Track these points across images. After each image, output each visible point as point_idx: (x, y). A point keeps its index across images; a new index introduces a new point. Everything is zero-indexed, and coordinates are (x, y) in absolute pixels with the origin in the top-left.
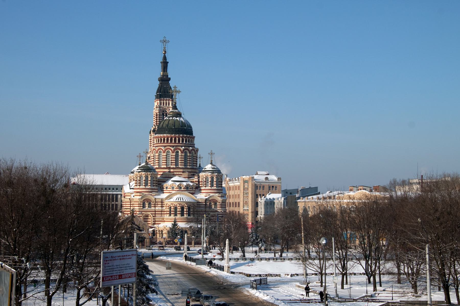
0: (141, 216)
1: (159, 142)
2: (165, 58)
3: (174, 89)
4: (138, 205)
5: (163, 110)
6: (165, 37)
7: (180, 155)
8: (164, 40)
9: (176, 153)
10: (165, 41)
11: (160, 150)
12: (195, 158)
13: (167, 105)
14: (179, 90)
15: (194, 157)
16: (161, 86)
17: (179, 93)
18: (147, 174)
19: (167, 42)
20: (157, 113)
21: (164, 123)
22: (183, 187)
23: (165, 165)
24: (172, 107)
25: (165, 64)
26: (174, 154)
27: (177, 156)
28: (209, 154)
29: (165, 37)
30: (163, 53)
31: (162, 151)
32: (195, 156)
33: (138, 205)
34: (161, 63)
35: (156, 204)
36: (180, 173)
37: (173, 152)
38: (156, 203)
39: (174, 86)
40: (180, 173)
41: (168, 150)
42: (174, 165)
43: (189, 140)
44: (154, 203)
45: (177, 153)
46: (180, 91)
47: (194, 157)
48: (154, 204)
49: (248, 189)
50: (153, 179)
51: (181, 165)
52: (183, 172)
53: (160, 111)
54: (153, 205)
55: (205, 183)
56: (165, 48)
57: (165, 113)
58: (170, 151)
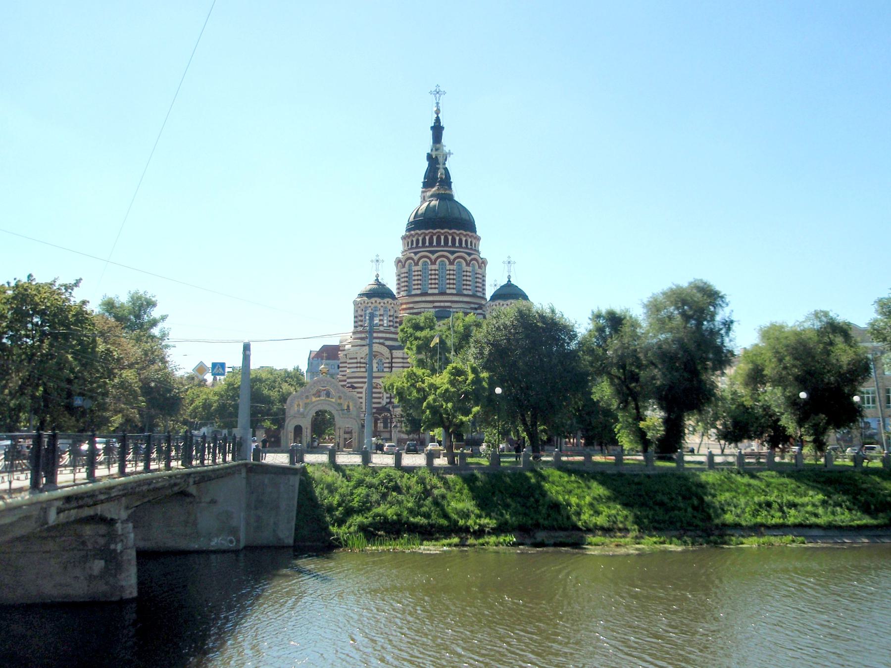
0: (362, 388)
2: (438, 120)
4: (355, 365)
8: (436, 91)
10: (438, 93)
12: (480, 276)
15: (476, 274)
18: (376, 302)
23: (417, 289)
25: (437, 130)
33: (355, 365)
35: (392, 363)
38: (393, 360)
42: (435, 288)
43: (466, 241)
44: (387, 361)
45: (442, 265)
47: (476, 274)
48: (389, 363)
50: (389, 313)
54: (387, 365)
56: (438, 103)
58: (428, 260)
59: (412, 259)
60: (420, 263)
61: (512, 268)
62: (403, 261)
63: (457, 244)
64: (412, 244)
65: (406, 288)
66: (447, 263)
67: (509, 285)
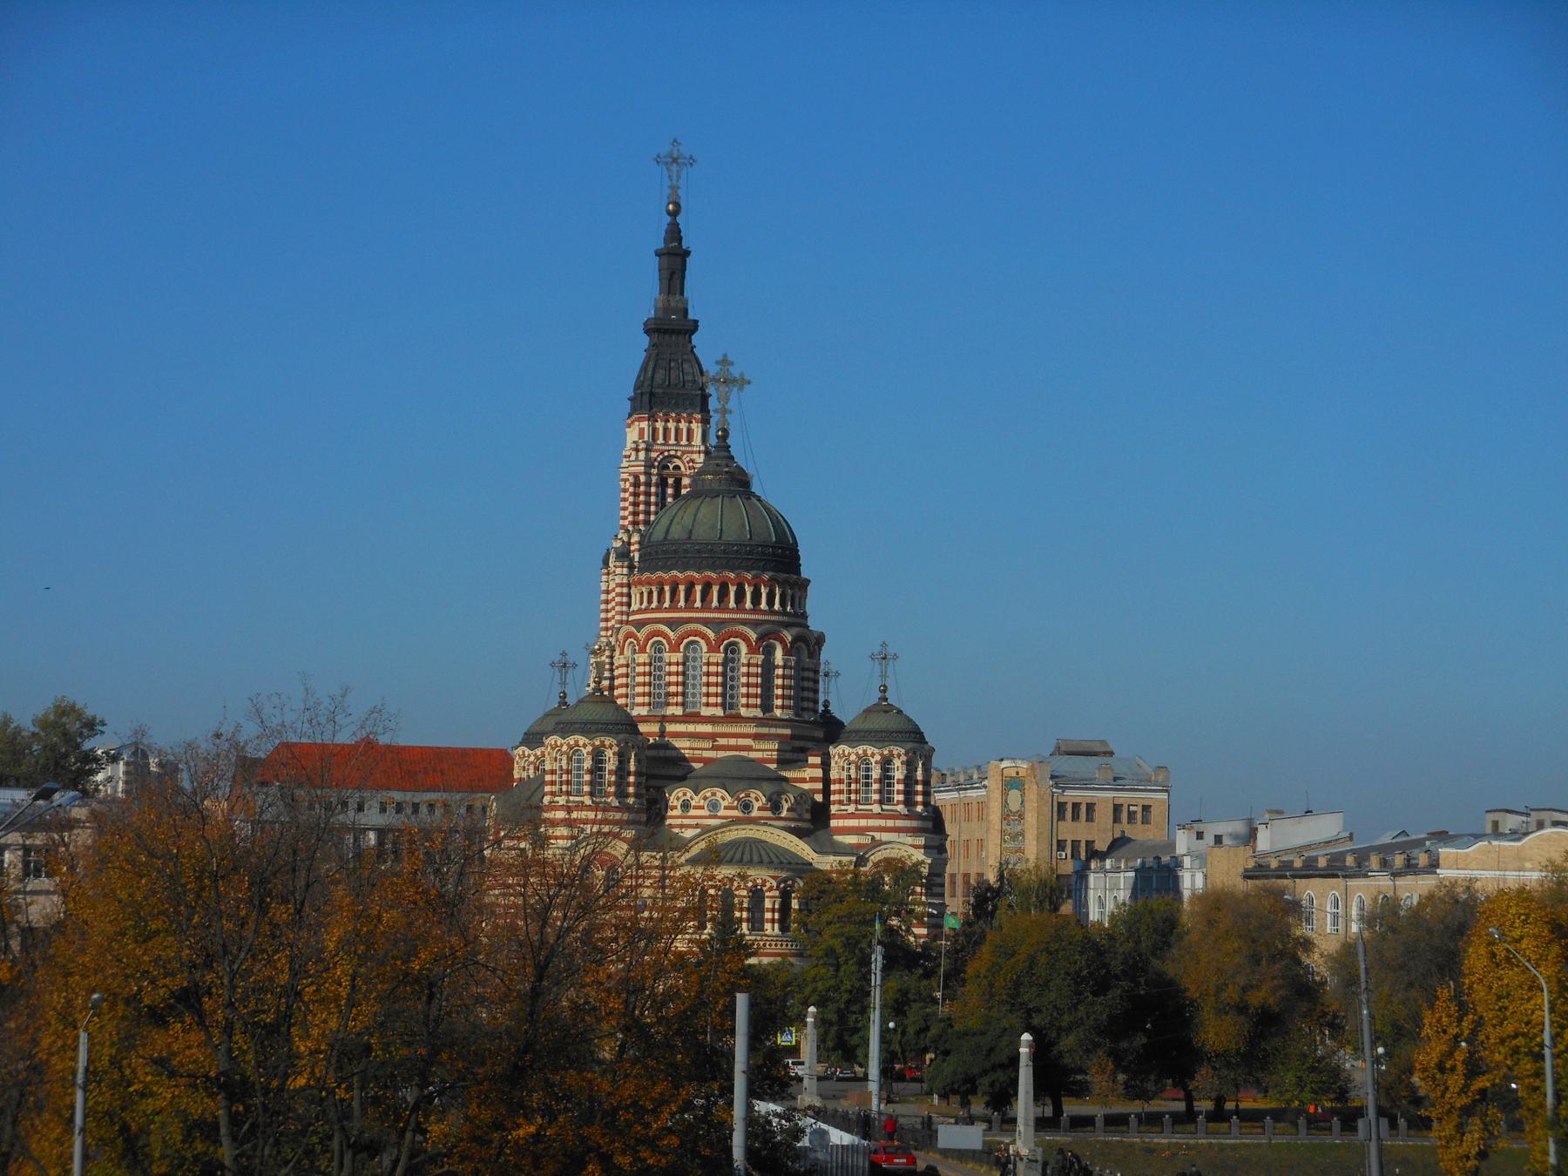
1: (650, 601)
2: (674, 233)
3: (718, 367)
5: (663, 463)
6: (675, 141)
7: (744, 660)
9: (726, 653)
10: (675, 160)
11: (655, 639)
12: (811, 675)
13: (684, 442)
14: (742, 374)
15: (804, 669)
16: (657, 355)
17: (741, 389)
19: (686, 165)
20: (636, 477)
21: (674, 517)
22: (757, 805)
24: (702, 448)
25: (674, 259)
26: (719, 657)
27: (729, 662)
28: (872, 657)
29: (675, 141)
30: (669, 213)
31: (664, 641)
32: (811, 666)
34: (658, 254)
36: (742, 742)
37: (713, 649)
39: (720, 358)
40: (742, 742)
41: (691, 638)
42: (716, 705)
45: (733, 652)
46: (747, 377)
47: (804, 669)
49: (1021, 816)
51: (748, 706)
52: (756, 737)
53: (649, 464)
55: (853, 786)
56: (674, 188)
57: (672, 476)
58: (703, 643)
59: (666, 636)
60: (682, 647)
61: (890, 668)
62: (641, 635)
63: (763, 606)
64: (661, 600)
65: (647, 699)
66: (744, 648)
67: (884, 707)
